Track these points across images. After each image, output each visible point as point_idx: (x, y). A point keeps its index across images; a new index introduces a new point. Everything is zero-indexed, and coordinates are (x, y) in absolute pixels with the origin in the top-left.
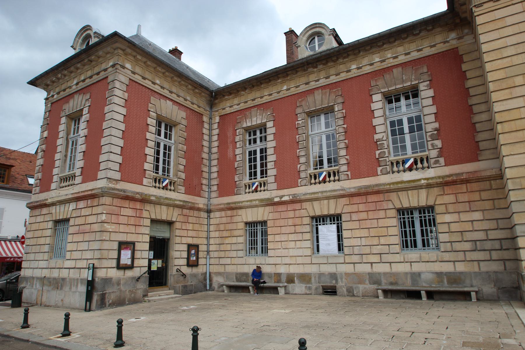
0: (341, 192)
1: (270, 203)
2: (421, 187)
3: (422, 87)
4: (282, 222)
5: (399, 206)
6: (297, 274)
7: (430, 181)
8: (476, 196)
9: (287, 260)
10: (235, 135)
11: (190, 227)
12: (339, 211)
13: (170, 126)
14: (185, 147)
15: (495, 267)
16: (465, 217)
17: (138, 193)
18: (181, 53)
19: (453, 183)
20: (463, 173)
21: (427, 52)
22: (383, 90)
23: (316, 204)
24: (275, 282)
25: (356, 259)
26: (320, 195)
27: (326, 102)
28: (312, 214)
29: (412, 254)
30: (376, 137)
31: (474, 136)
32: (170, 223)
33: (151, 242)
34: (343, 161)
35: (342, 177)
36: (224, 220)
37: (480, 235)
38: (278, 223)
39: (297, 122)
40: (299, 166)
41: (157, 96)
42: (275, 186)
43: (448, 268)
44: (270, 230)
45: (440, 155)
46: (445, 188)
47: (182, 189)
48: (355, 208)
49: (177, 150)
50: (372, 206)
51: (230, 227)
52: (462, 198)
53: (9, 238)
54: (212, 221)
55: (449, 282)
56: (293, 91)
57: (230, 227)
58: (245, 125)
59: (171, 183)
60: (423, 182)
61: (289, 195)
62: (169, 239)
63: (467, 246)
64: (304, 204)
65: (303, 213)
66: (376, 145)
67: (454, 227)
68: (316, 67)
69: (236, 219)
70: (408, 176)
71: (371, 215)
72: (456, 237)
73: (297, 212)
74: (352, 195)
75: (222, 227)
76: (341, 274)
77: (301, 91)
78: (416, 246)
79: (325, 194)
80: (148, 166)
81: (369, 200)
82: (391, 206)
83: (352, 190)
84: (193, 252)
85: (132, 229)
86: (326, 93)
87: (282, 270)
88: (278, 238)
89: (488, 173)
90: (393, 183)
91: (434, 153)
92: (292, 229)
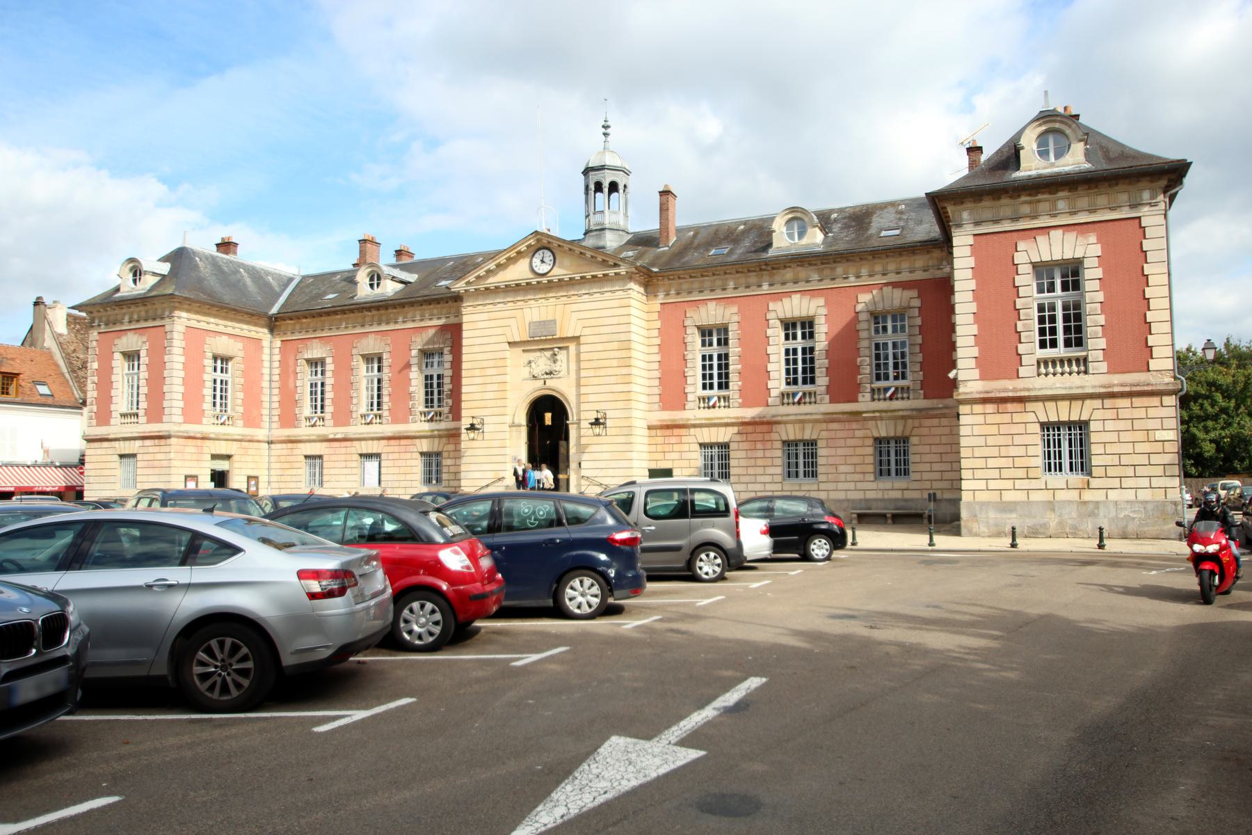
3: (446, 350)
7: (440, 433)
10: (296, 365)
11: (250, 459)
13: (226, 360)
14: (242, 380)
17: (199, 433)
18: (235, 245)
22: (419, 347)
26: (365, 436)
30: (411, 389)
32: (228, 457)
33: (212, 475)
34: (385, 407)
35: (384, 421)
36: (285, 452)
41: (212, 334)
44: (325, 465)
45: (450, 412)
46: (451, 439)
47: (240, 423)
48: (390, 449)
49: (233, 384)
50: (403, 449)
51: (290, 459)
53: (29, 463)
54: (273, 453)
57: (290, 459)
58: (306, 357)
59: (228, 418)
60: (436, 432)
62: (228, 471)
65: (353, 450)
66: (410, 396)
69: (296, 452)
71: (403, 456)
75: (283, 459)
79: (370, 436)
80: (207, 405)
84: (253, 482)
85: (195, 464)
88: (332, 471)
90: (417, 432)
92: (343, 464)
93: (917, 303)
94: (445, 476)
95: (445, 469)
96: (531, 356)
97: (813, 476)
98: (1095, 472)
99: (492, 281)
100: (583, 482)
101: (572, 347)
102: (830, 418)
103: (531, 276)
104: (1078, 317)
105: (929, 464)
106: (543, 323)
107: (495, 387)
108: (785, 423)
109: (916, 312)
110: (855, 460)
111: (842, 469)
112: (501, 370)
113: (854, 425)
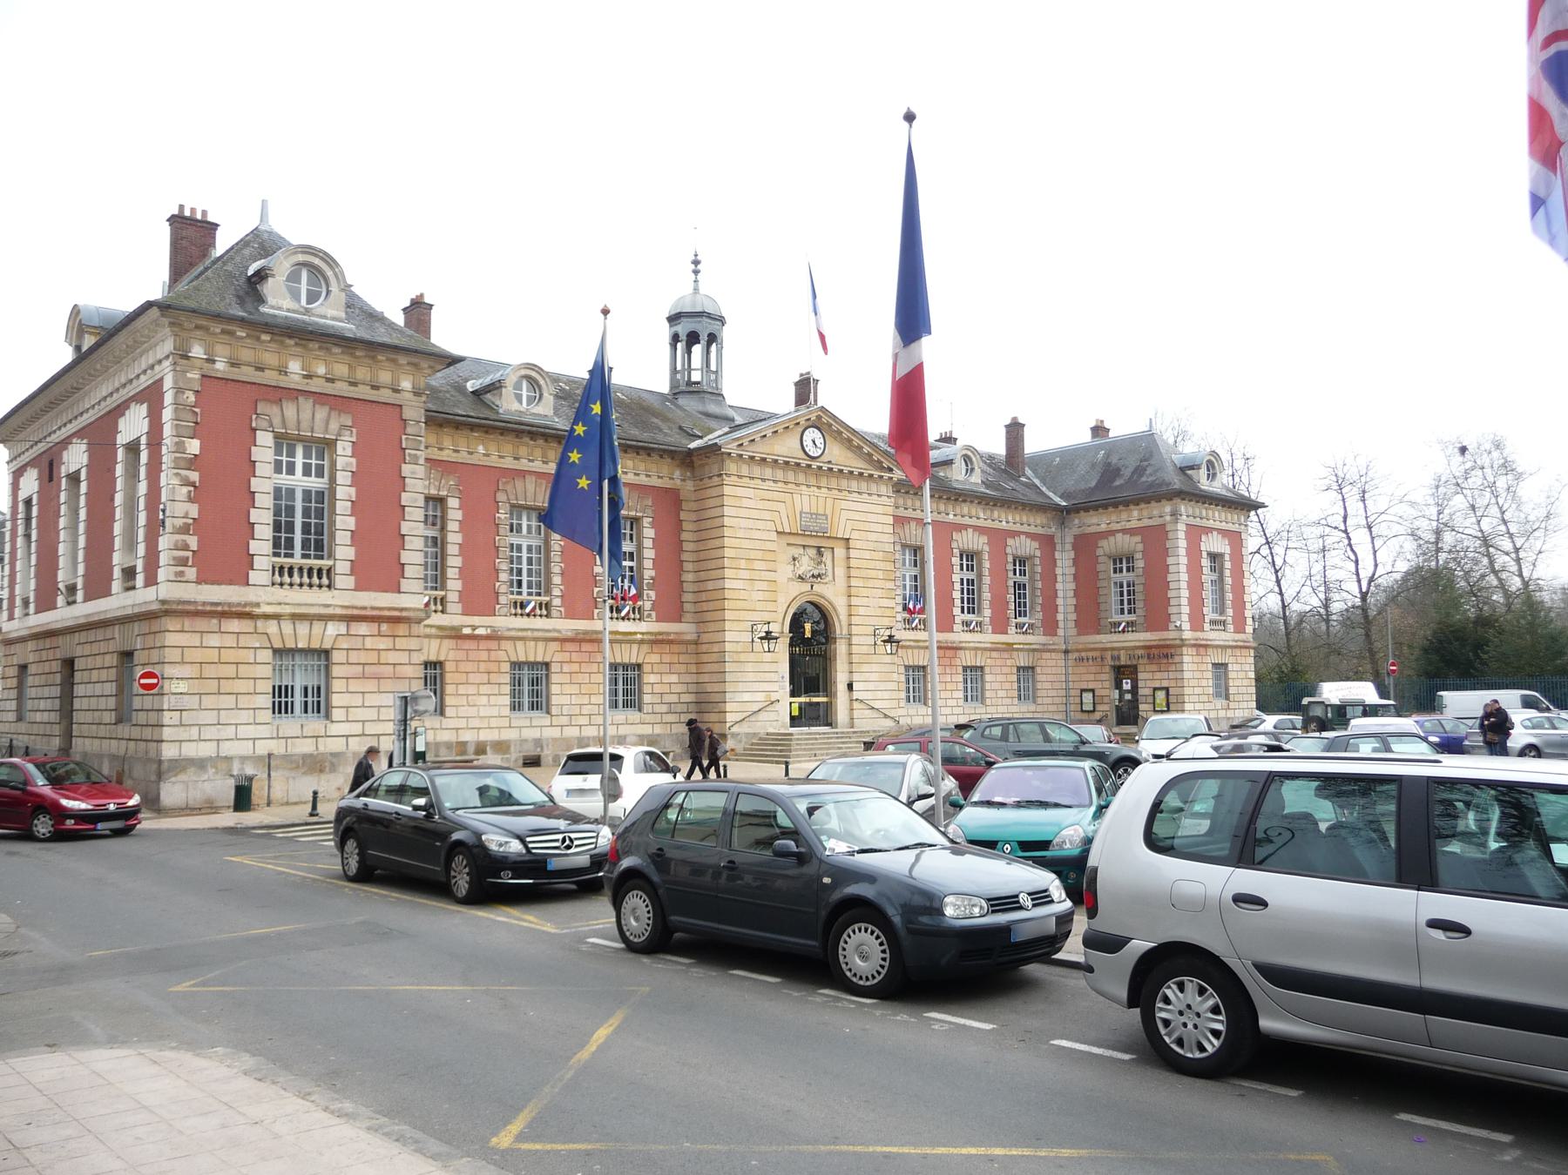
0: (556, 635)
1: (455, 634)
2: (633, 642)
3: (646, 522)
4: (470, 667)
6: (491, 742)
7: (645, 637)
9: (475, 723)
12: (547, 659)
16: (666, 679)
19: (661, 642)
21: (655, 482)
23: (519, 644)
24: (457, 755)
25: (564, 720)
27: (541, 500)
28: (514, 659)
34: (556, 592)
35: (554, 613)
37: (674, 698)
38: (462, 667)
40: (498, 584)
42: (458, 608)
50: (585, 657)
52: (667, 658)
56: (494, 461)
60: (639, 636)
63: (664, 708)
65: (502, 655)
67: (657, 688)
72: (657, 699)
73: (493, 653)
74: (564, 640)
76: (547, 739)
81: (583, 650)
83: (569, 634)
86: (541, 484)
87: (467, 736)
88: (462, 689)
89: (688, 637)
91: (648, 605)
93: (1038, 553)
94: (647, 698)
95: (647, 689)
96: (797, 551)
97: (534, 706)
98: (337, 714)
99: (760, 450)
100: (856, 705)
101: (840, 552)
103: (802, 455)
104: (320, 514)
105: (460, 692)
107: (764, 586)
108: (965, 649)
109: (1037, 561)
110: (1007, 686)
112: (771, 566)
113: (1006, 655)
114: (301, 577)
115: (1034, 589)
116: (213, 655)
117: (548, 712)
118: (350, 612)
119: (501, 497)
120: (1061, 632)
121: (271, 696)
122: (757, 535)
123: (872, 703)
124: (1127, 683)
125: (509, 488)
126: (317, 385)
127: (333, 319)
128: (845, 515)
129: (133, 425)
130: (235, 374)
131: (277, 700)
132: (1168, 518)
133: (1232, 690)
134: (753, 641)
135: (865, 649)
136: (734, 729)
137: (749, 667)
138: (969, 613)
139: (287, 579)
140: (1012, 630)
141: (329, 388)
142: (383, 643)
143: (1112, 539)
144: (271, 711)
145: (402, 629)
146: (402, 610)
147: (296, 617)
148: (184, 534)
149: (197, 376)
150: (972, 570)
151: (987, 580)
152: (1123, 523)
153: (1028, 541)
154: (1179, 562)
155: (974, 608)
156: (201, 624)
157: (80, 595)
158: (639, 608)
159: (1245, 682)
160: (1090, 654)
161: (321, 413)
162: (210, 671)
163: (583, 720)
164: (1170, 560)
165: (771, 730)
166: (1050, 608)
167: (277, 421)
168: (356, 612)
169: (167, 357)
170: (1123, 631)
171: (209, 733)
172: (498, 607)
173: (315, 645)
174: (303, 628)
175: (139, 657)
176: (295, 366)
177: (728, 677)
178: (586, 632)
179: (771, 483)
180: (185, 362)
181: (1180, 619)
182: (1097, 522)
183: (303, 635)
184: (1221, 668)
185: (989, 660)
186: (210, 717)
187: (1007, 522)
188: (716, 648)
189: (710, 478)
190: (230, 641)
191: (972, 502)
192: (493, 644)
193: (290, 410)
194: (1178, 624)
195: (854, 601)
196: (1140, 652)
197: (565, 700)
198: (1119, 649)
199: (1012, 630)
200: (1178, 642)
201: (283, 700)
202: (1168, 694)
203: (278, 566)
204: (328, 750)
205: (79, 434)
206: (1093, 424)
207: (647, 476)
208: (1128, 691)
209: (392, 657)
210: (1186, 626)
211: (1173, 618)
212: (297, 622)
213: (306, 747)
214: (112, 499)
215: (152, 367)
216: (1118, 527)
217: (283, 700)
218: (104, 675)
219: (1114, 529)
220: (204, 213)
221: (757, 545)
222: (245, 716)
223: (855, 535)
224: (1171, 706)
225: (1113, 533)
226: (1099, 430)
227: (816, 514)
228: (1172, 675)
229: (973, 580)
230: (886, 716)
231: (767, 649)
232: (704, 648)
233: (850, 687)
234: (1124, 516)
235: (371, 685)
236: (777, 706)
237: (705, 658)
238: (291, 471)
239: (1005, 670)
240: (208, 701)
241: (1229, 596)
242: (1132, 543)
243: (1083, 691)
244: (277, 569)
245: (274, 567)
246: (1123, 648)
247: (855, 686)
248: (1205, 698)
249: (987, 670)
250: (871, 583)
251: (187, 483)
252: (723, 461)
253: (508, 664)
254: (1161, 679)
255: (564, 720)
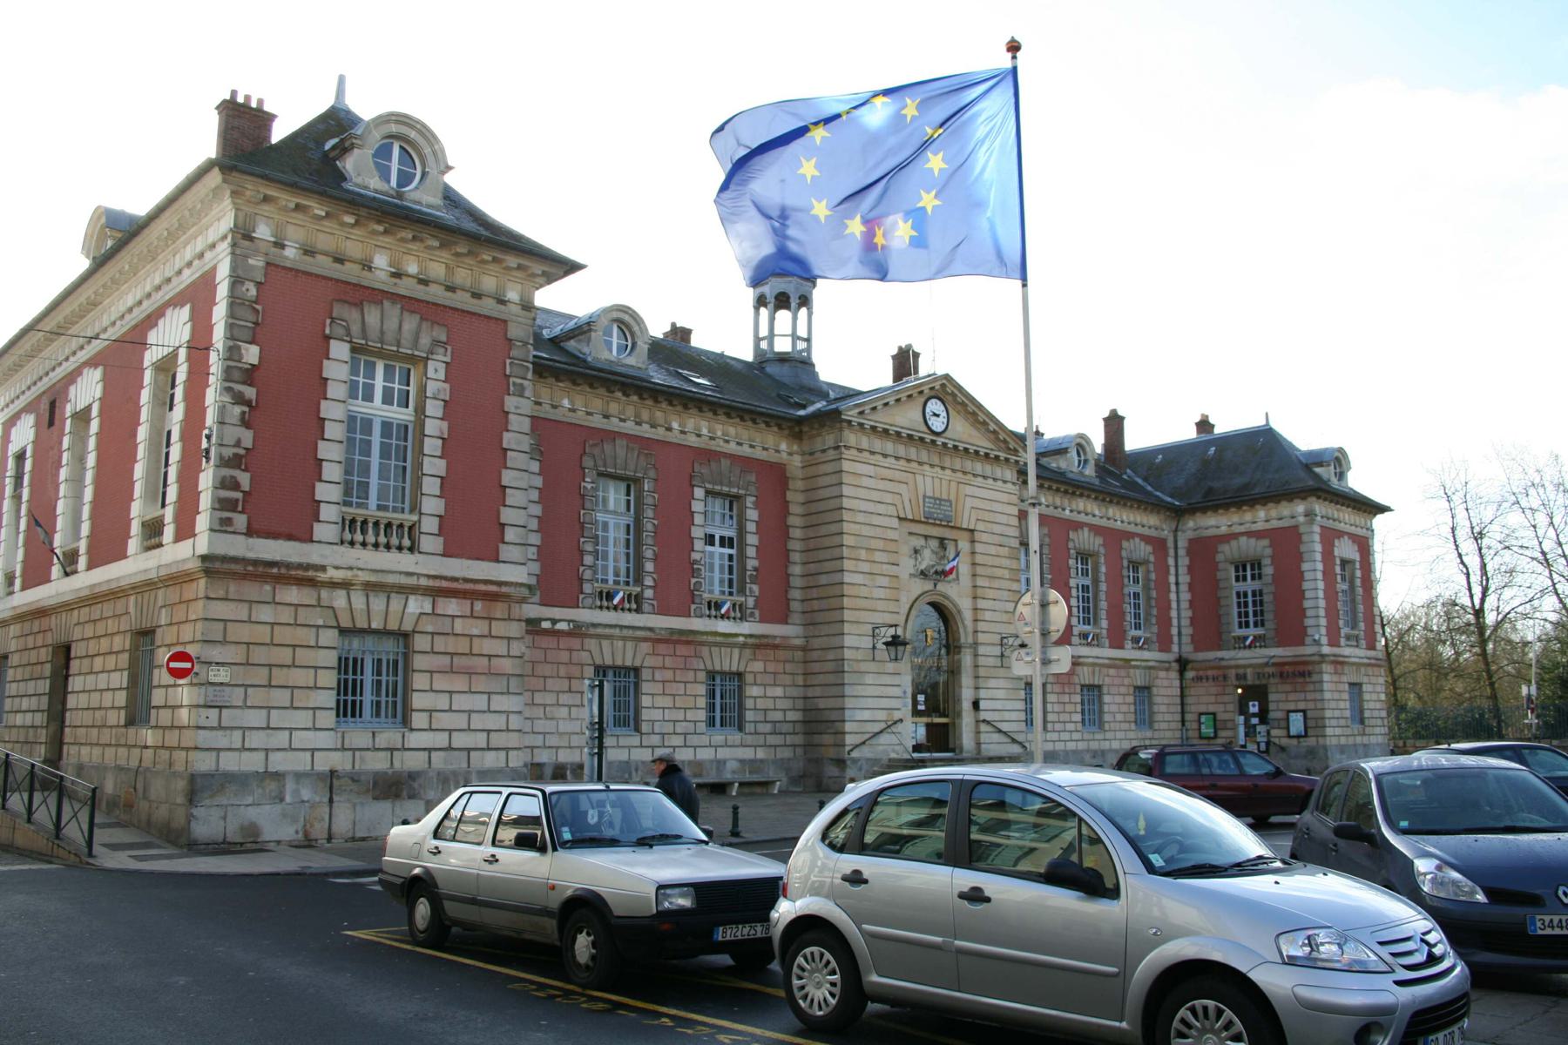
3: (750, 501)
4: (547, 670)
5: (710, 667)
6: (572, 764)
8: (780, 668)
9: (553, 741)
15: (786, 753)
16: (771, 692)
19: (767, 646)
20: (775, 637)
22: (707, 486)
25: (655, 740)
28: (599, 662)
29: (718, 738)
31: (786, 591)
34: (649, 581)
35: (646, 607)
37: (778, 716)
39: (583, 484)
43: (748, 754)
46: (757, 651)
48: (658, 661)
52: (771, 667)
55: (750, 772)
56: (580, 418)
60: (741, 639)
61: (569, 621)
63: (768, 728)
64: (587, 641)
67: (761, 704)
68: (628, 396)
70: (724, 626)
73: (574, 653)
76: (636, 762)
77: (593, 425)
78: (714, 726)
82: (703, 667)
91: (751, 602)
93: (1152, 558)
94: (749, 716)
95: (749, 703)
96: (919, 542)
100: (983, 727)
101: (964, 545)
102: (1114, 664)
106: (938, 501)
107: (884, 581)
109: (1152, 567)
110: (1124, 708)
111: (1119, 717)
112: (892, 557)
113: (1123, 672)
114: (377, 535)
115: (1149, 598)
116: (263, 633)
117: (637, 729)
118: (437, 583)
119: (588, 462)
120: (1175, 648)
121: (335, 692)
122: (876, 520)
123: (999, 725)
124: (1254, 706)
125: (596, 451)
126: (406, 287)
127: (429, 206)
128: (969, 502)
129: (173, 332)
130: (309, 264)
131: (342, 698)
132: (1302, 519)
133: (1367, 714)
134: (874, 648)
135: (991, 661)
136: (854, 754)
137: (869, 679)
138: (1084, 624)
139: (359, 537)
140: (1129, 644)
141: (420, 292)
142: (478, 628)
143: (1234, 543)
144: (334, 712)
145: (499, 609)
146: (500, 584)
147: (370, 588)
148: (233, 467)
149: (261, 264)
150: (1087, 575)
151: (1103, 587)
152: (1248, 525)
153: (1143, 544)
154: (1313, 569)
155: (1089, 618)
156: (252, 590)
157: (82, 562)
158: (741, 606)
159: (1378, 705)
160: (1210, 673)
161: (410, 323)
162: (259, 655)
163: (677, 741)
164: (1305, 566)
165: (893, 755)
166: (1165, 622)
167: (355, 329)
168: (445, 584)
169: (224, 237)
170: (1250, 647)
171: (255, 740)
172: (581, 596)
173: (393, 625)
174: (378, 603)
175: (165, 636)
176: (381, 261)
177: (848, 690)
178: (681, 632)
179: (892, 460)
180: (247, 243)
181: (1319, 632)
182: (1216, 523)
183: (377, 613)
184: (1356, 687)
185: (1106, 678)
186: (255, 718)
187: (1122, 522)
188: (831, 655)
189: (824, 451)
190: (286, 615)
191: (1088, 497)
192: (575, 643)
193: (372, 316)
194: (1317, 637)
195: (981, 604)
196: (1270, 670)
197: (657, 715)
198: (1245, 667)
199: (1129, 644)
200: (1316, 658)
201: (350, 698)
202: (1305, 718)
203: (348, 518)
204: (406, 768)
205: (92, 363)
206: (1198, 420)
207: (752, 446)
208: (1254, 715)
209: (488, 646)
210: (1324, 640)
211: (1310, 631)
212: (371, 594)
213: (377, 763)
214: (135, 435)
215: (201, 256)
216: (1242, 529)
217: (350, 698)
218: (111, 662)
219: (1237, 531)
220: (260, 102)
221: (878, 532)
222: (303, 719)
223: (980, 526)
224: (1309, 730)
225: (1235, 536)
226: (1204, 425)
227: (940, 500)
228: (1310, 696)
229: (1088, 587)
230: (1014, 741)
231: (893, 657)
232: (815, 655)
233: (976, 705)
234: (1248, 517)
235: (460, 683)
236: (899, 728)
237: (816, 667)
238: (369, 397)
239: (1123, 690)
240: (255, 696)
241: (1361, 608)
242: (1261, 548)
243: (1201, 714)
244: (347, 522)
245: (343, 519)
246: (1250, 666)
247: (982, 705)
248: (1342, 722)
249: (1105, 690)
250: (996, 584)
251: (239, 399)
252: (841, 430)
253: (592, 668)
254: (1296, 700)
255: (655, 740)
